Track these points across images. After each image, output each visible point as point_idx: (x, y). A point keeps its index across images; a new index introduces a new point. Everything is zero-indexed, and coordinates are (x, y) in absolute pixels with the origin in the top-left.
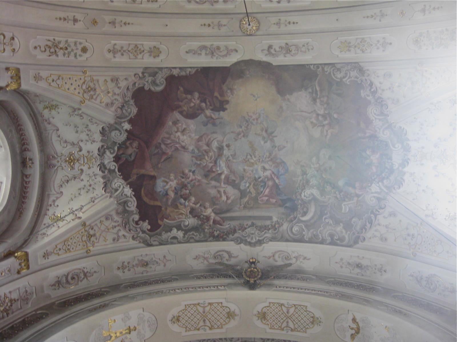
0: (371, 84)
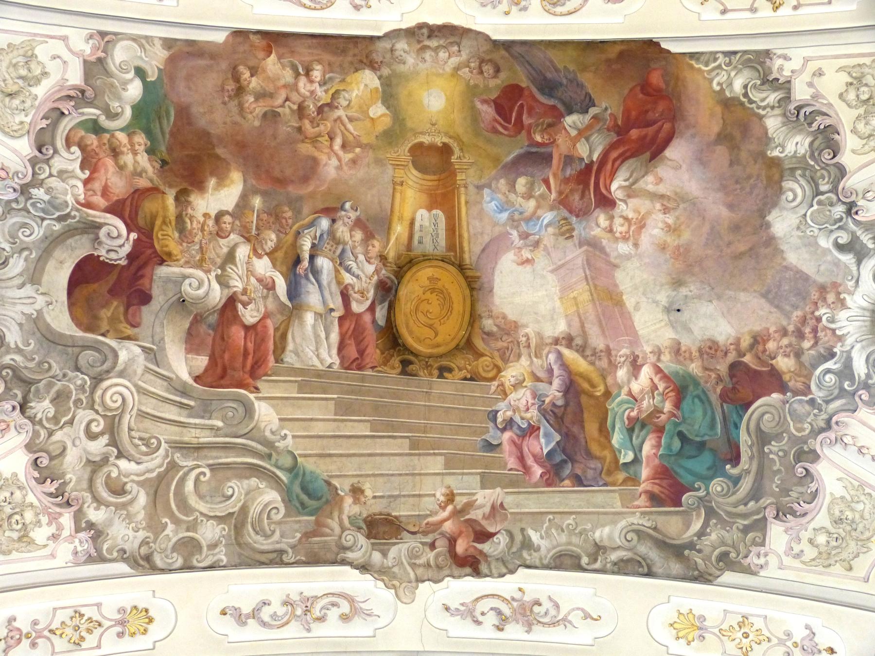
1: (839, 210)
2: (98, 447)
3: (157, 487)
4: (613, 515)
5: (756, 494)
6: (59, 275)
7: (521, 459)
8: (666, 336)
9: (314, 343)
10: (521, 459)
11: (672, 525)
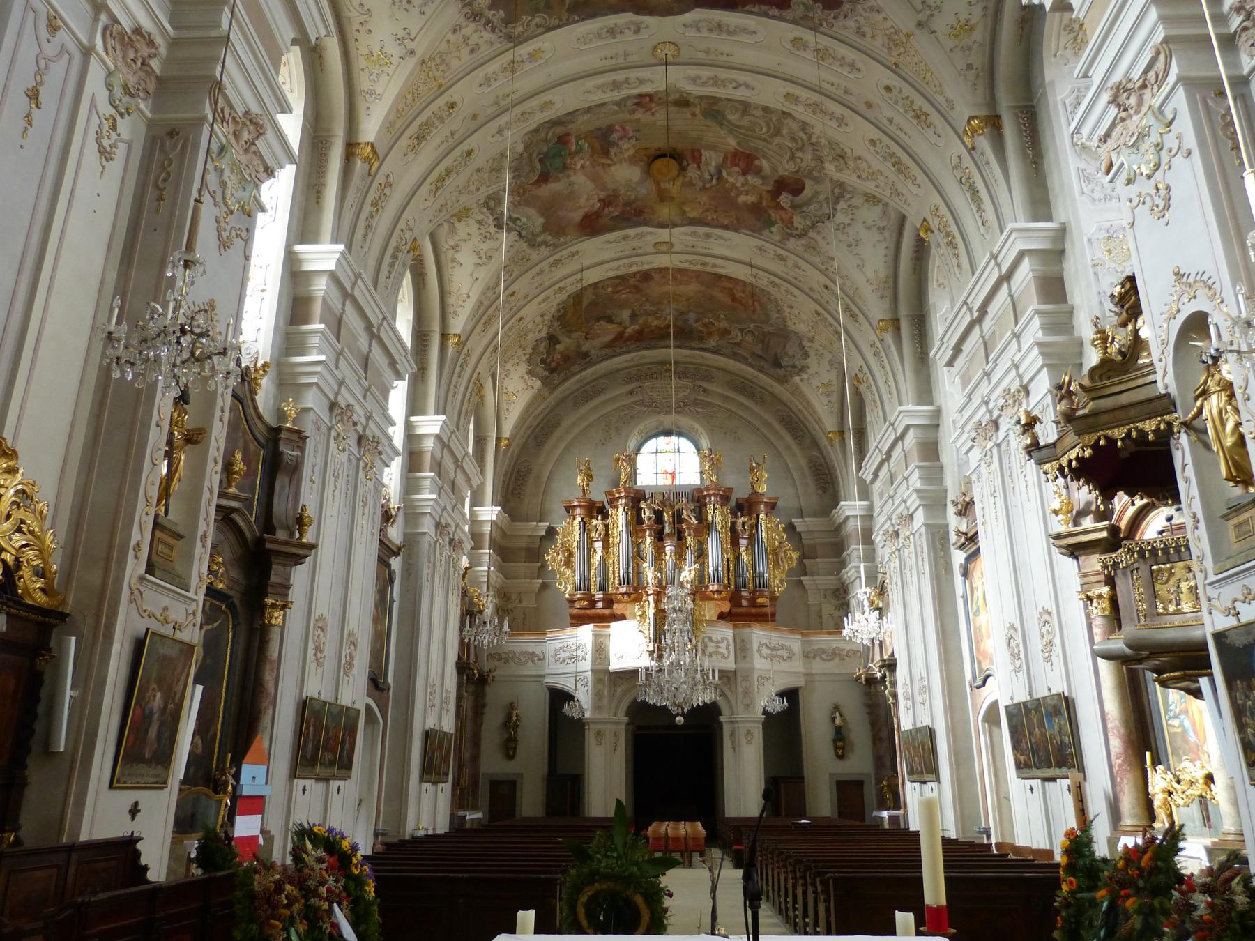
0: (493, 30)
1: (524, 233)
2: (798, 154)
3: (778, 132)
4: (584, 124)
5: (530, 155)
6: (807, 192)
7: (623, 129)
8: (573, 178)
9: (712, 159)
10: (623, 129)
11: (559, 130)
